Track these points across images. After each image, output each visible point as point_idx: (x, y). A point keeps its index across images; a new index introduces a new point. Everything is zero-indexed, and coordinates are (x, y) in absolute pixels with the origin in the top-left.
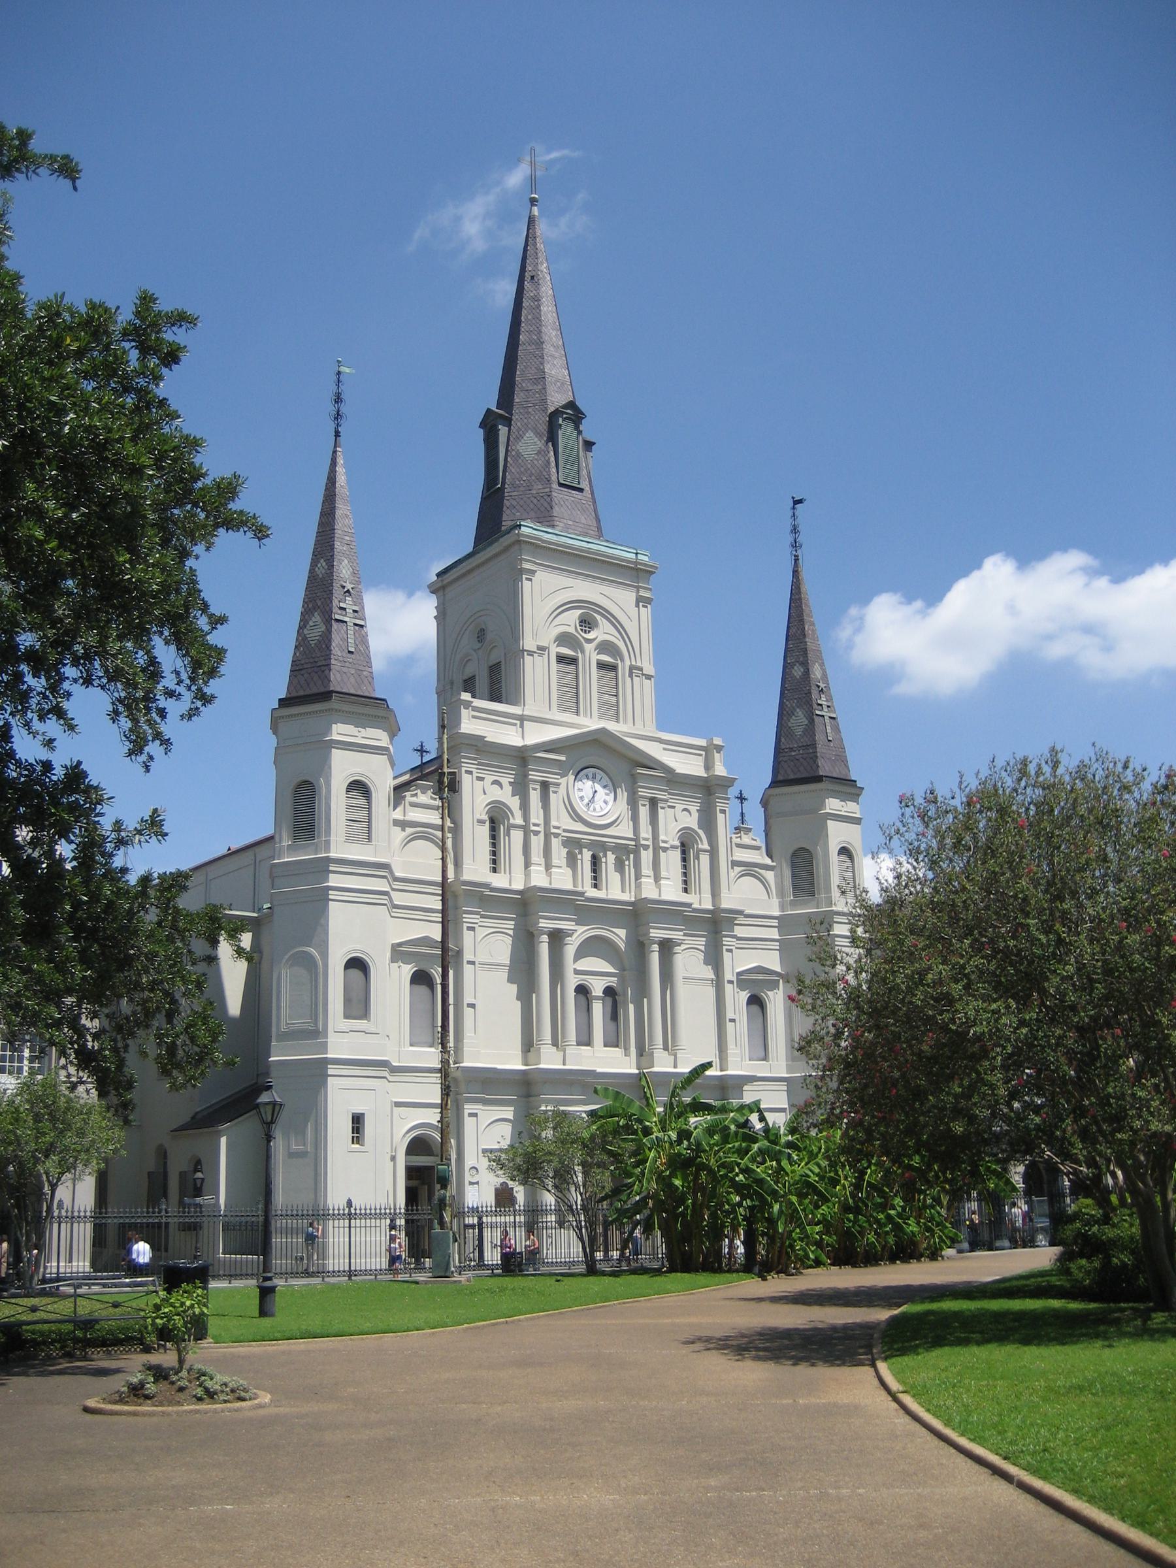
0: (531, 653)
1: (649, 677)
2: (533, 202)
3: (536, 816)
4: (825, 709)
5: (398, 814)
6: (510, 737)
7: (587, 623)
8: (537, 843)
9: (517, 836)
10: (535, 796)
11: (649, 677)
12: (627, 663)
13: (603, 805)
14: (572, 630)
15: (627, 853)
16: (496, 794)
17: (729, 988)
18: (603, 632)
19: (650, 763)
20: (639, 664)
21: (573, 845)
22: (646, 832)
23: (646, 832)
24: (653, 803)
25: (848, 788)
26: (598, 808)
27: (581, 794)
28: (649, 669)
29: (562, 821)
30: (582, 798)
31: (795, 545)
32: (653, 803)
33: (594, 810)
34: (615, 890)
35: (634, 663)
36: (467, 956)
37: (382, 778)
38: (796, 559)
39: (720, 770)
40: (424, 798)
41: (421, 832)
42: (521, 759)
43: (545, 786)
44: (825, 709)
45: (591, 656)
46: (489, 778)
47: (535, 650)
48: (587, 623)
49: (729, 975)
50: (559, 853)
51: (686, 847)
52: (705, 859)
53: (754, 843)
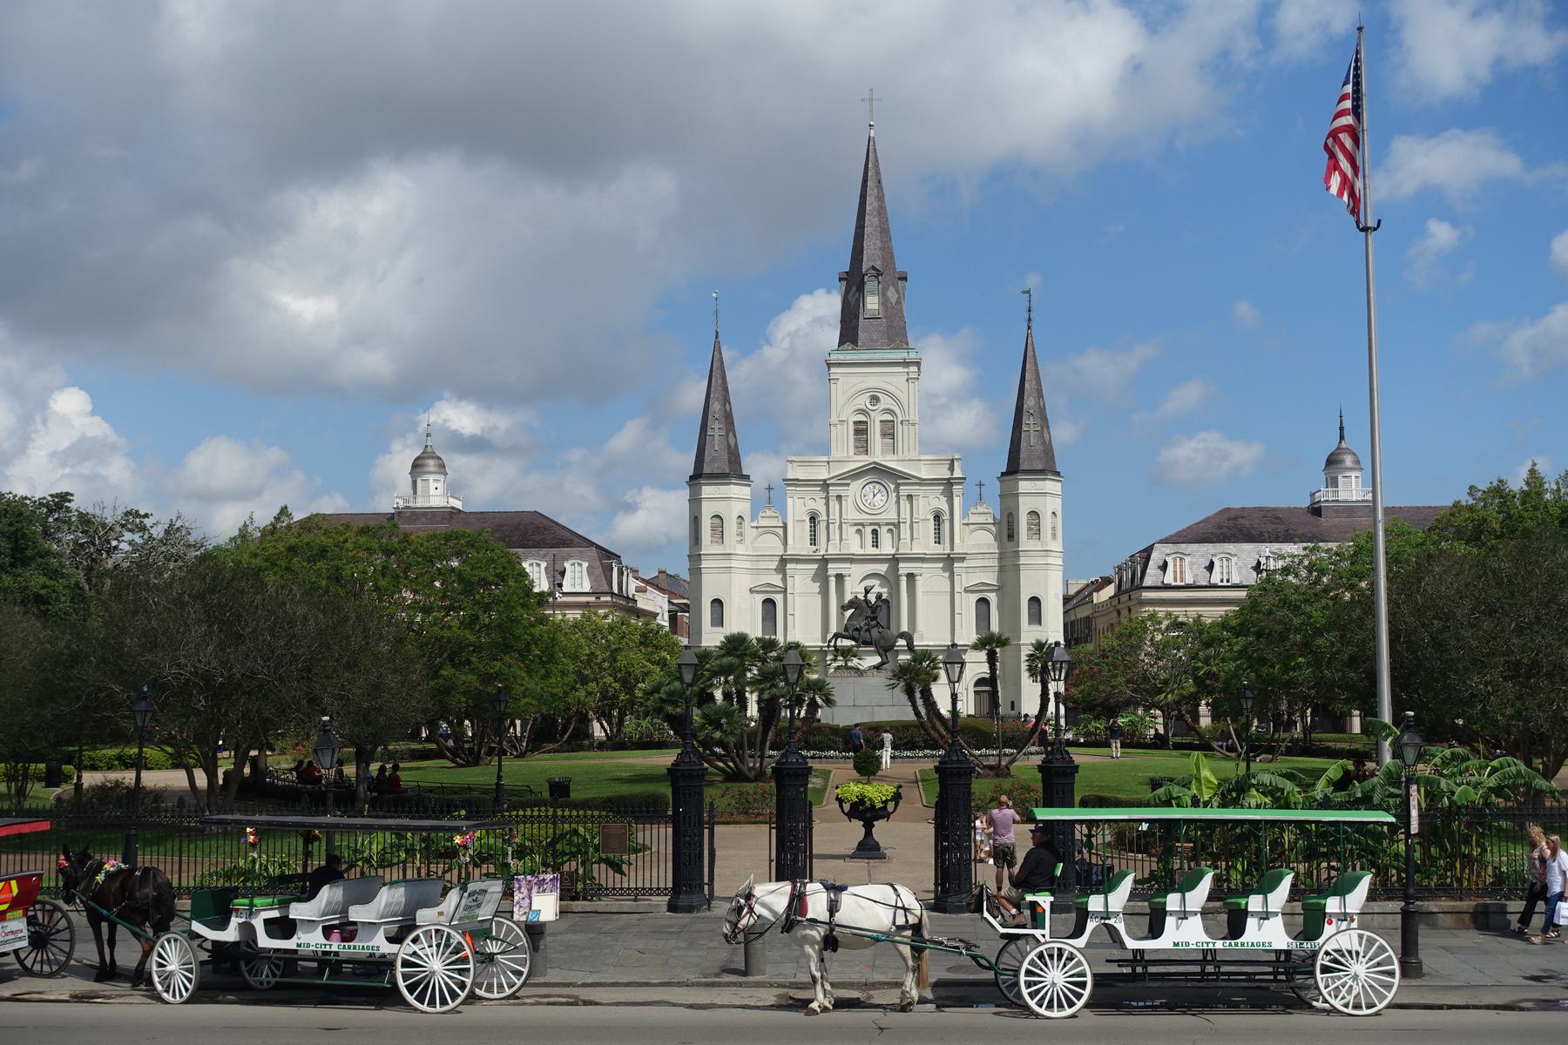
0: (835, 425)
1: (914, 424)
2: (870, 126)
3: (835, 515)
5: (755, 524)
6: (823, 474)
7: (875, 399)
8: (834, 529)
9: (823, 526)
10: (834, 504)
11: (914, 424)
12: (900, 419)
14: (865, 408)
16: (811, 505)
17: (957, 596)
18: (886, 402)
19: (905, 476)
21: (859, 527)
22: (905, 514)
23: (905, 514)
24: (910, 497)
25: (1047, 470)
26: (876, 504)
28: (914, 417)
29: (851, 514)
31: (1029, 320)
32: (910, 497)
34: (887, 548)
36: (789, 591)
37: (744, 508)
39: (958, 473)
40: (769, 513)
41: (768, 530)
42: (825, 485)
43: (839, 498)
45: (877, 418)
46: (807, 498)
47: (837, 422)
48: (875, 399)
49: (957, 589)
50: (850, 532)
51: (937, 518)
52: (947, 525)
53: (987, 511)
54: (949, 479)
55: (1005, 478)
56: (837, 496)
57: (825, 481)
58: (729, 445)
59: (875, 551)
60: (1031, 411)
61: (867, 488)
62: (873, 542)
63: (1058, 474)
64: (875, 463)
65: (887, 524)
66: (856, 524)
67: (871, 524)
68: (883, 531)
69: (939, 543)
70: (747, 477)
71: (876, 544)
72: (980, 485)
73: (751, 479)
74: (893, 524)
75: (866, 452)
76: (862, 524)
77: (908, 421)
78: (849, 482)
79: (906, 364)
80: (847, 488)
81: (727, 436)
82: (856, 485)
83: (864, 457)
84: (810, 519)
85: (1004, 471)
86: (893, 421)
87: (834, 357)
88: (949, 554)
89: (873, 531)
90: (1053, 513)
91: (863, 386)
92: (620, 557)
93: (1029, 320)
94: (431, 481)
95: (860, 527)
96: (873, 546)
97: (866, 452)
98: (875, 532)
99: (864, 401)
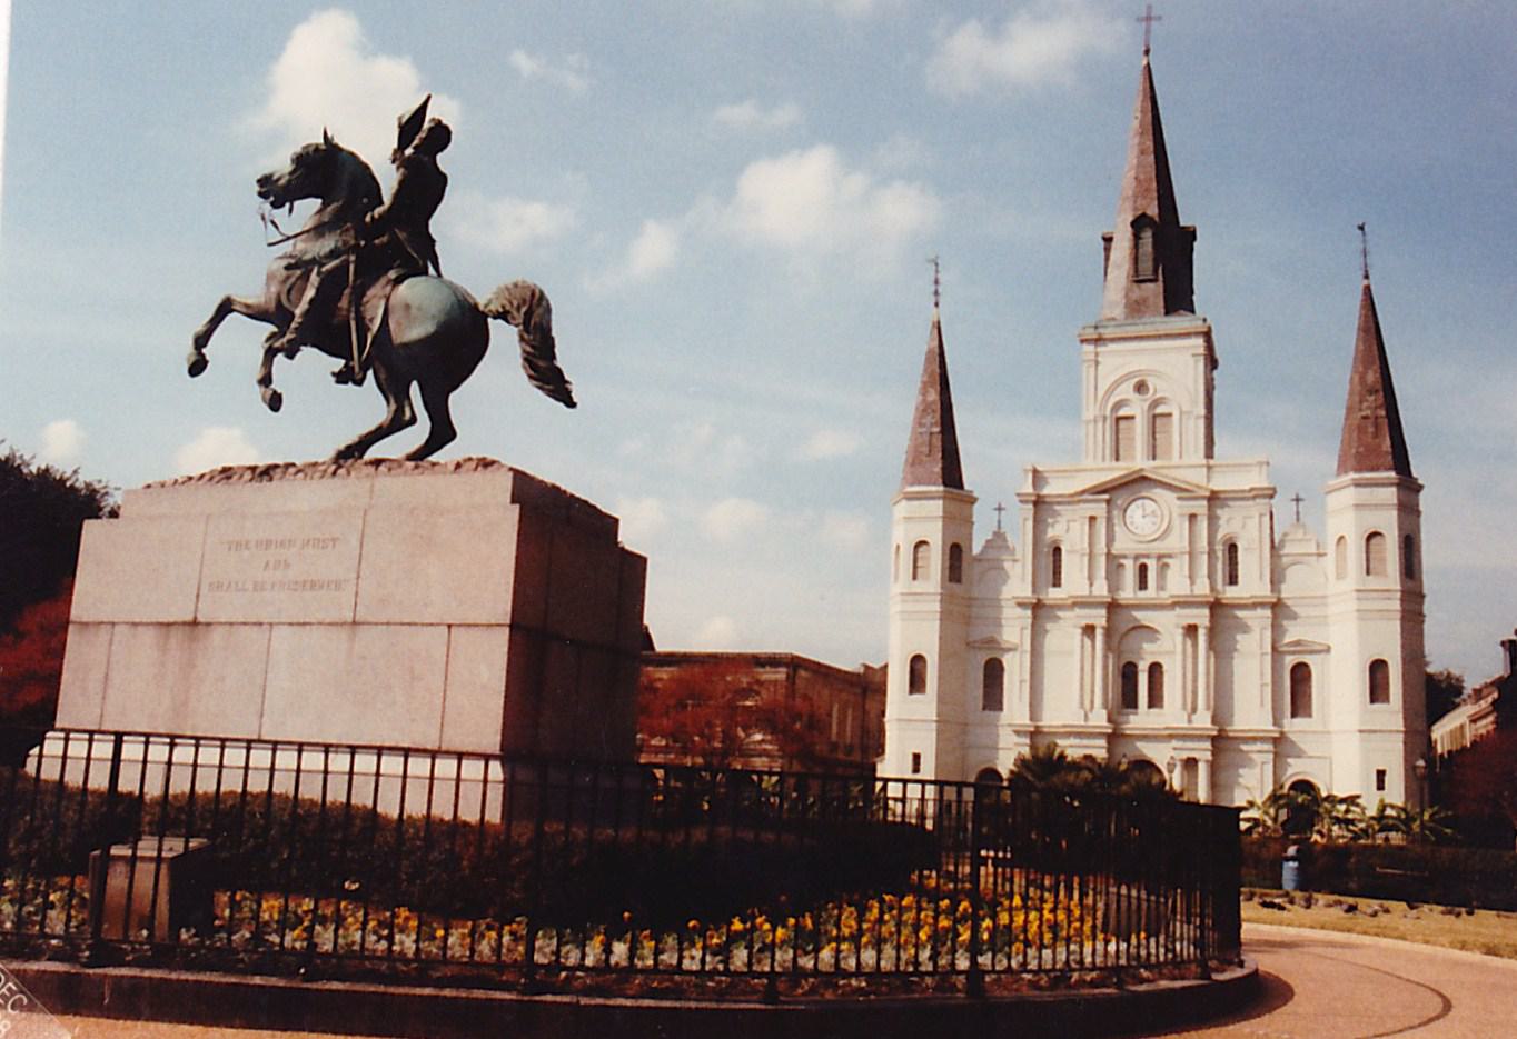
7: (1141, 387)
11: (1198, 417)
18: (1156, 386)
24: (1192, 517)
30: (1132, 523)
31: (1366, 266)
43: (1092, 519)
48: (1141, 387)
54: (1252, 490)
62: (1140, 582)
65: (1160, 557)
67: (1137, 557)
68: (1152, 564)
71: (1143, 585)
72: (1298, 500)
74: (1170, 556)
75: (1133, 458)
76: (1125, 557)
78: (1106, 496)
79: (1188, 335)
86: (1170, 415)
87: (1091, 333)
93: (1366, 266)
98: (1143, 569)
99: (1127, 390)
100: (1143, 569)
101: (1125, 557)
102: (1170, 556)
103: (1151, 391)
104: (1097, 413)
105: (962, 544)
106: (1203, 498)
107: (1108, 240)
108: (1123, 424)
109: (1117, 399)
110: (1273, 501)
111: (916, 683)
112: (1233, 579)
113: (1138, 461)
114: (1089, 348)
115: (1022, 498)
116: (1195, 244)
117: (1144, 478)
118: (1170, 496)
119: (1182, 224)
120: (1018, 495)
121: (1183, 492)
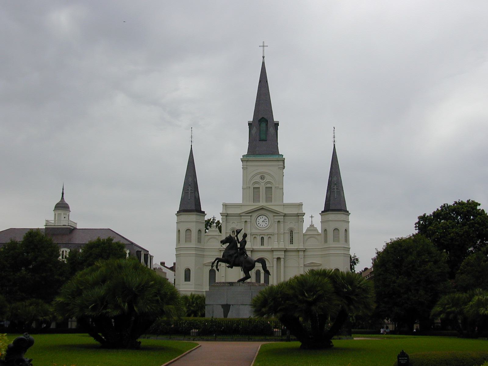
4: (336, 190)
7: (262, 178)
13: (265, 224)
15: (270, 236)
18: (268, 178)
20: (278, 186)
26: (263, 225)
27: (259, 222)
30: (259, 223)
31: (334, 141)
33: (262, 226)
35: (276, 186)
38: (334, 145)
42: (240, 215)
44: (336, 190)
48: (262, 178)
54: (297, 214)
55: (322, 214)
56: (245, 221)
57: (240, 214)
58: (195, 197)
59: (262, 247)
60: (335, 183)
61: (259, 218)
62: (262, 243)
63: (348, 212)
64: (262, 206)
66: (253, 235)
68: (266, 238)
69: (292, 244)
70: (204, 212)
71: (262, 244)
73: (205, 213)
74: (271, 235)
75: (259, 201)
76: (257, 235)
77: (278, 187)
78: (250, 215)
80: (250, 217)
81: (195, 193)
82: (255, 215)
83: (256, 204)
84: (233, 232)
85: (323, 210)
87: (246, 159)
88: (297, 249)
89: (262, 238)
90: (346, 230)
91: (259, 171)
92: (148, 251)
93: (334, 141)
94: (62, 214)
95: (256, 236)
96: (262, 245)
97: (259, 201)
98: (262, 238)
99: (257, 179)
100: (262, 238)
101: (257, 235)
102: (271, 235)
103: (264, 181)
104: (247, 186)
105: (202, 230)
106: (282, 216)
107: (250, 124)
108: (256, 190)
109: (254, 181)
110: (304, 217)
111: (187, 278)
112: (292, 242)
113: (262, 203)
114: (245, 163)
115: (222, 215)
116: (278, 127)
117: (262, 209)
118: (271, 215)
119: (275, 120)
120: (220, 213)
121: (276, 213)
